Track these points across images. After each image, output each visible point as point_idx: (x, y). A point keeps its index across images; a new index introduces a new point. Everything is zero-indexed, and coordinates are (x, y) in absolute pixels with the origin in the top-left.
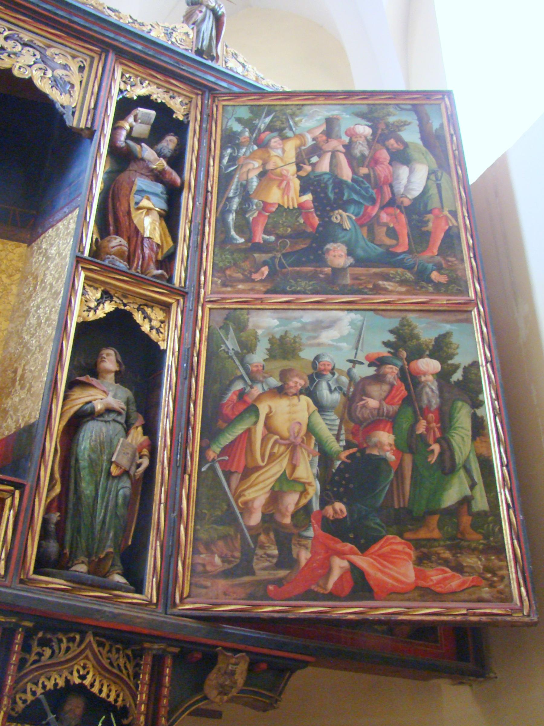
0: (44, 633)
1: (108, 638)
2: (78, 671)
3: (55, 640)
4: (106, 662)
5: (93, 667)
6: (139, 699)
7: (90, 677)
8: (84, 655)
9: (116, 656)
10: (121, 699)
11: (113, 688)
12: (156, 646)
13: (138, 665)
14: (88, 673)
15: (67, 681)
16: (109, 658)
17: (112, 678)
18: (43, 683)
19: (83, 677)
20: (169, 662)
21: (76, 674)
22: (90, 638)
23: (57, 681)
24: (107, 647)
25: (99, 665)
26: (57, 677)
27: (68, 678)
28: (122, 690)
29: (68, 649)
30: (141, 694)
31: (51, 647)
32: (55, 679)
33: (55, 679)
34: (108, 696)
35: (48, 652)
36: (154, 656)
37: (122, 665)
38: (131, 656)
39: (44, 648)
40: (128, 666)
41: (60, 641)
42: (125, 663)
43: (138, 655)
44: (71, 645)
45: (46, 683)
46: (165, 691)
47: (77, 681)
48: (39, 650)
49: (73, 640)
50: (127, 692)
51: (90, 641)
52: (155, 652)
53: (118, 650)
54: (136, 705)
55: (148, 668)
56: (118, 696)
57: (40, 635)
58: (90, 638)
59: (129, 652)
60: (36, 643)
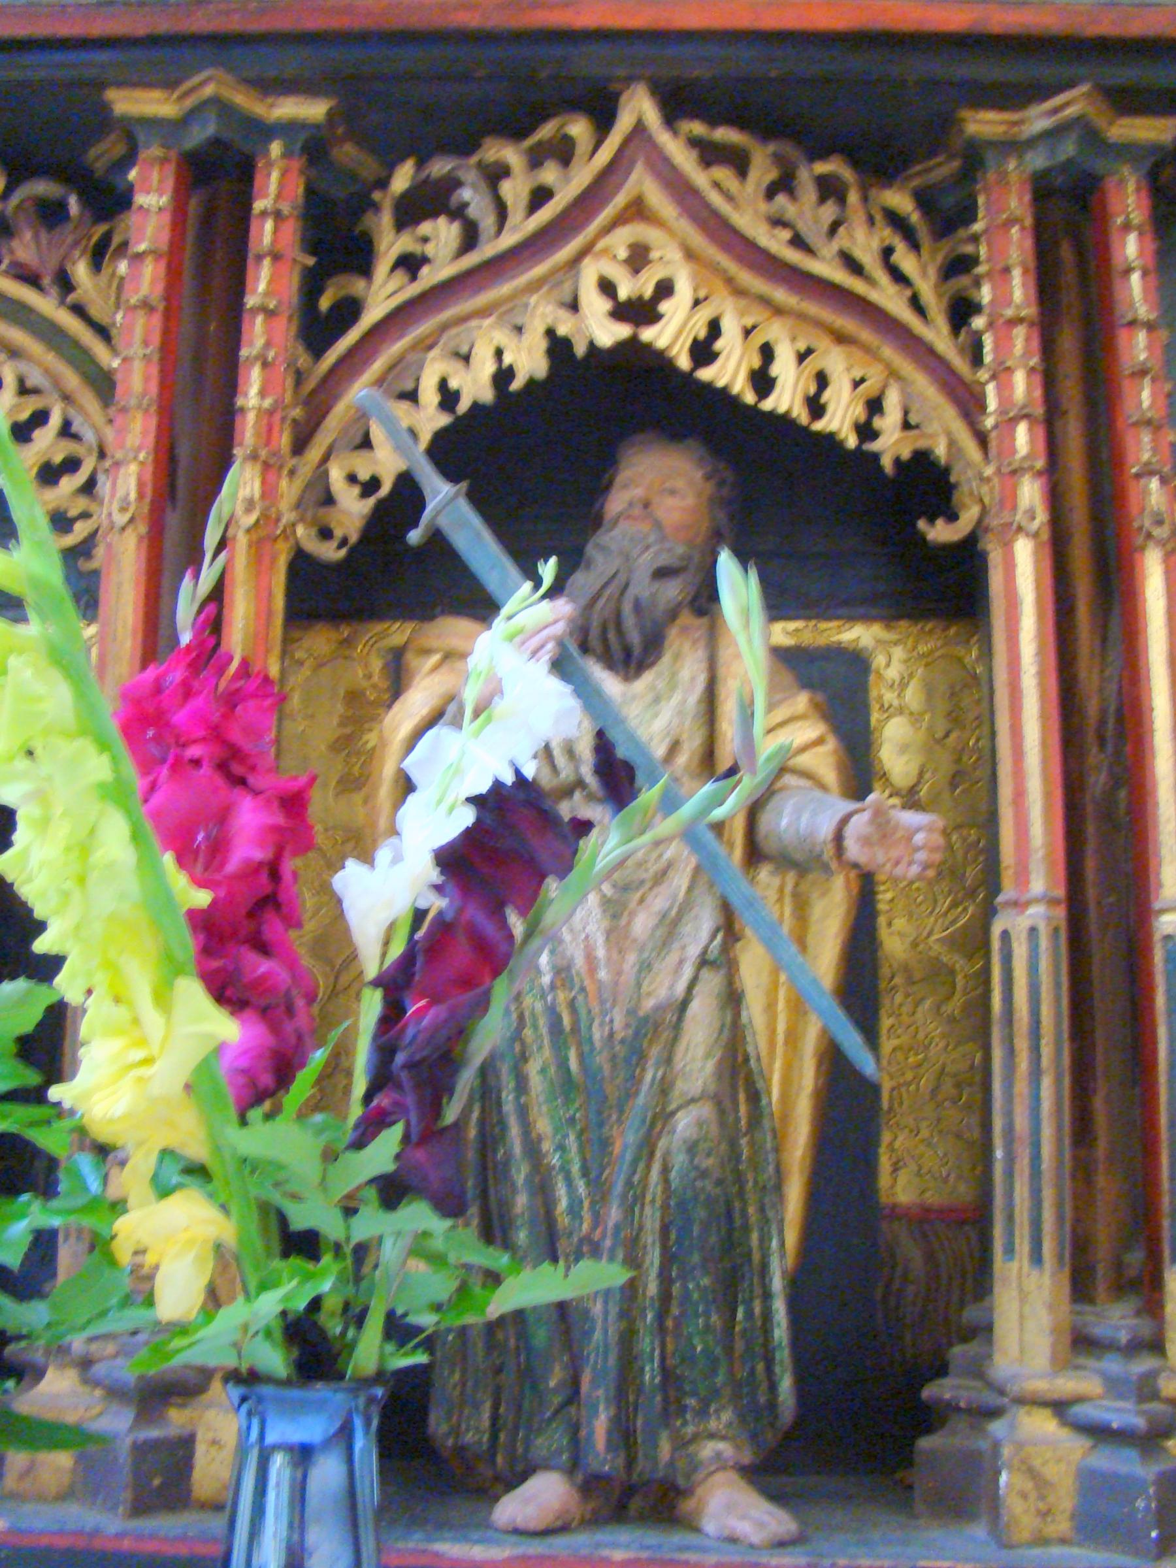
0: (420, 164)
1: (766, 126)
2: (607, 287)
3: (470, 175)
4: (776, 243)
5: (690, 255)
6: (992, 404)
7: (675, 309)
8: (620, 200)
9: (829, 211)
10: (889, 422)
11: (836, 363)
12: (1037, 119)
13: (958, 266)
14: (665, 289)
15: (558, 347)
16: (778, 222)
17: (813, 308)
18: (443, 385)
19: (640, 312)
20: (1129, 201)
21: (595, 305)
22: (639, 107)
23: (507, 359)
24: (762, 171)
25: (726, 247)
26: (501, 337)
27: (562, 331)
28: (893, 374)
29: (540, 196)
30: (1002, 373)
31: (458, 213)
32: (499, 353)
33: (499, 353)
34: (816, 408)
35: (442, 234)
36: (1043, 190)
37: (868, 257)
38: (915, 218)
39: (425, 228)
40: (906, 261)
41: (496, 174)
42: (887, 252)
43: (948, 214)
44: (549, 174)
45: (453, 384)
46: (1138, 348)
47: (608, 333)
48: (405, 243)
49: (564, 152)
50: (923, 384)
51: (639, 128)
52: (1037, 160)
53: (829, 189)
54: (982, 439)
55: (1018, 246)
56: (875, 406)
57: (402, 179)
58: (639, 107)
59: (900, 200)
60: (386, 219)
